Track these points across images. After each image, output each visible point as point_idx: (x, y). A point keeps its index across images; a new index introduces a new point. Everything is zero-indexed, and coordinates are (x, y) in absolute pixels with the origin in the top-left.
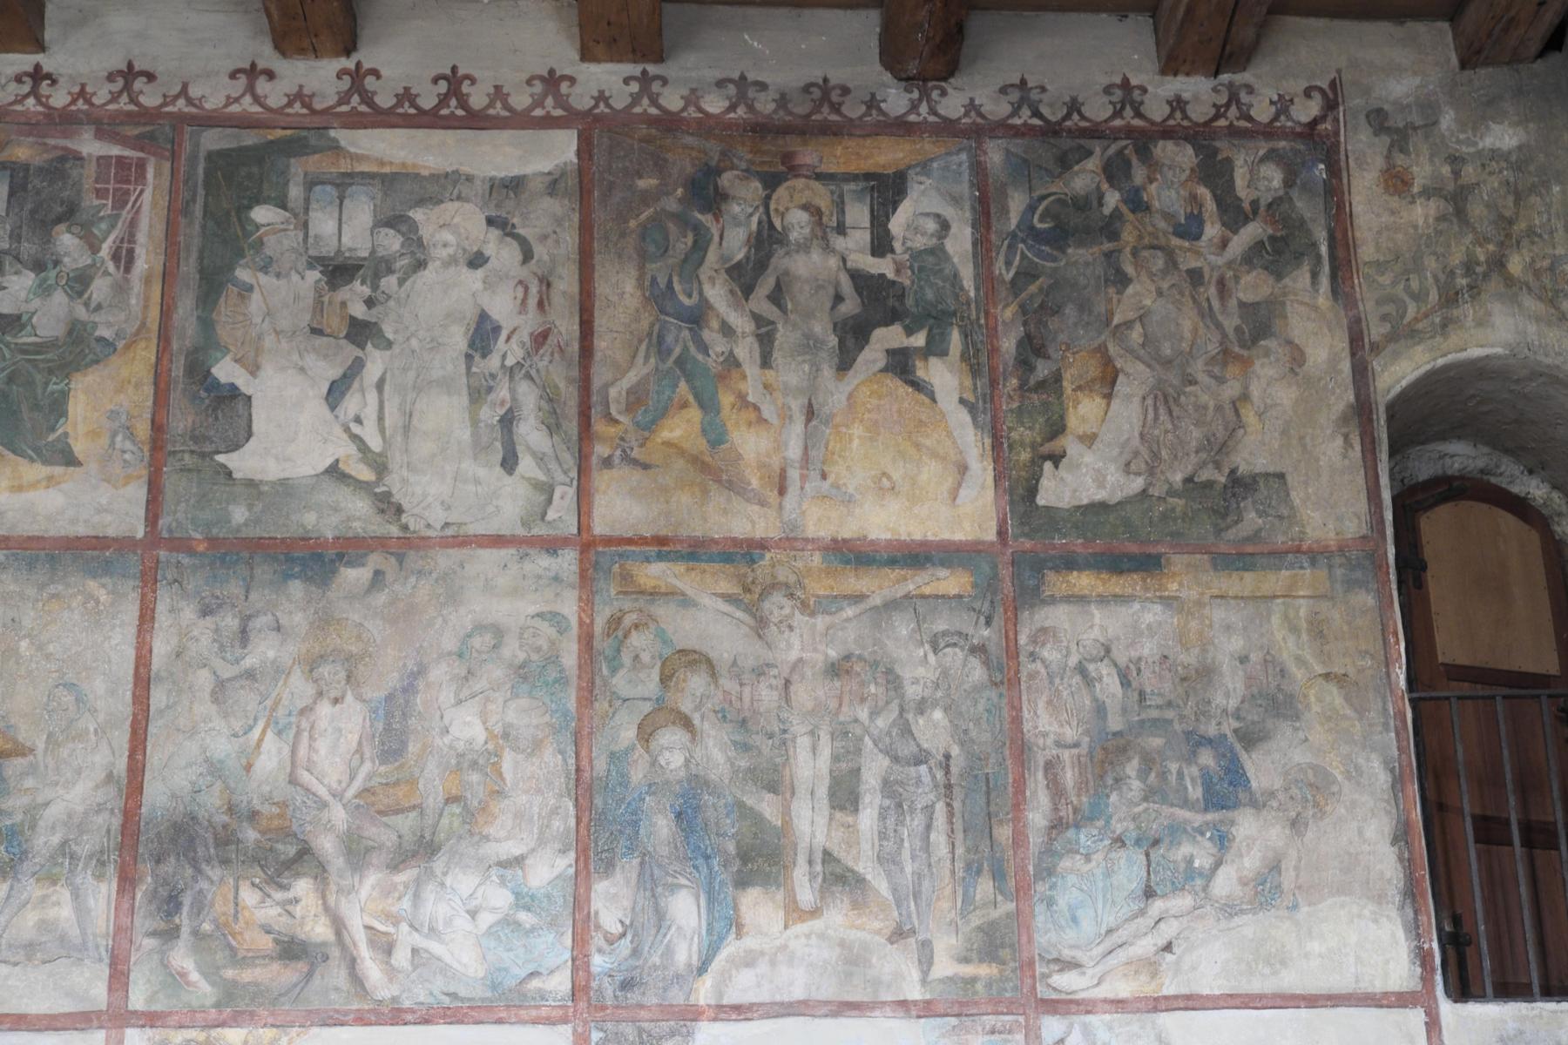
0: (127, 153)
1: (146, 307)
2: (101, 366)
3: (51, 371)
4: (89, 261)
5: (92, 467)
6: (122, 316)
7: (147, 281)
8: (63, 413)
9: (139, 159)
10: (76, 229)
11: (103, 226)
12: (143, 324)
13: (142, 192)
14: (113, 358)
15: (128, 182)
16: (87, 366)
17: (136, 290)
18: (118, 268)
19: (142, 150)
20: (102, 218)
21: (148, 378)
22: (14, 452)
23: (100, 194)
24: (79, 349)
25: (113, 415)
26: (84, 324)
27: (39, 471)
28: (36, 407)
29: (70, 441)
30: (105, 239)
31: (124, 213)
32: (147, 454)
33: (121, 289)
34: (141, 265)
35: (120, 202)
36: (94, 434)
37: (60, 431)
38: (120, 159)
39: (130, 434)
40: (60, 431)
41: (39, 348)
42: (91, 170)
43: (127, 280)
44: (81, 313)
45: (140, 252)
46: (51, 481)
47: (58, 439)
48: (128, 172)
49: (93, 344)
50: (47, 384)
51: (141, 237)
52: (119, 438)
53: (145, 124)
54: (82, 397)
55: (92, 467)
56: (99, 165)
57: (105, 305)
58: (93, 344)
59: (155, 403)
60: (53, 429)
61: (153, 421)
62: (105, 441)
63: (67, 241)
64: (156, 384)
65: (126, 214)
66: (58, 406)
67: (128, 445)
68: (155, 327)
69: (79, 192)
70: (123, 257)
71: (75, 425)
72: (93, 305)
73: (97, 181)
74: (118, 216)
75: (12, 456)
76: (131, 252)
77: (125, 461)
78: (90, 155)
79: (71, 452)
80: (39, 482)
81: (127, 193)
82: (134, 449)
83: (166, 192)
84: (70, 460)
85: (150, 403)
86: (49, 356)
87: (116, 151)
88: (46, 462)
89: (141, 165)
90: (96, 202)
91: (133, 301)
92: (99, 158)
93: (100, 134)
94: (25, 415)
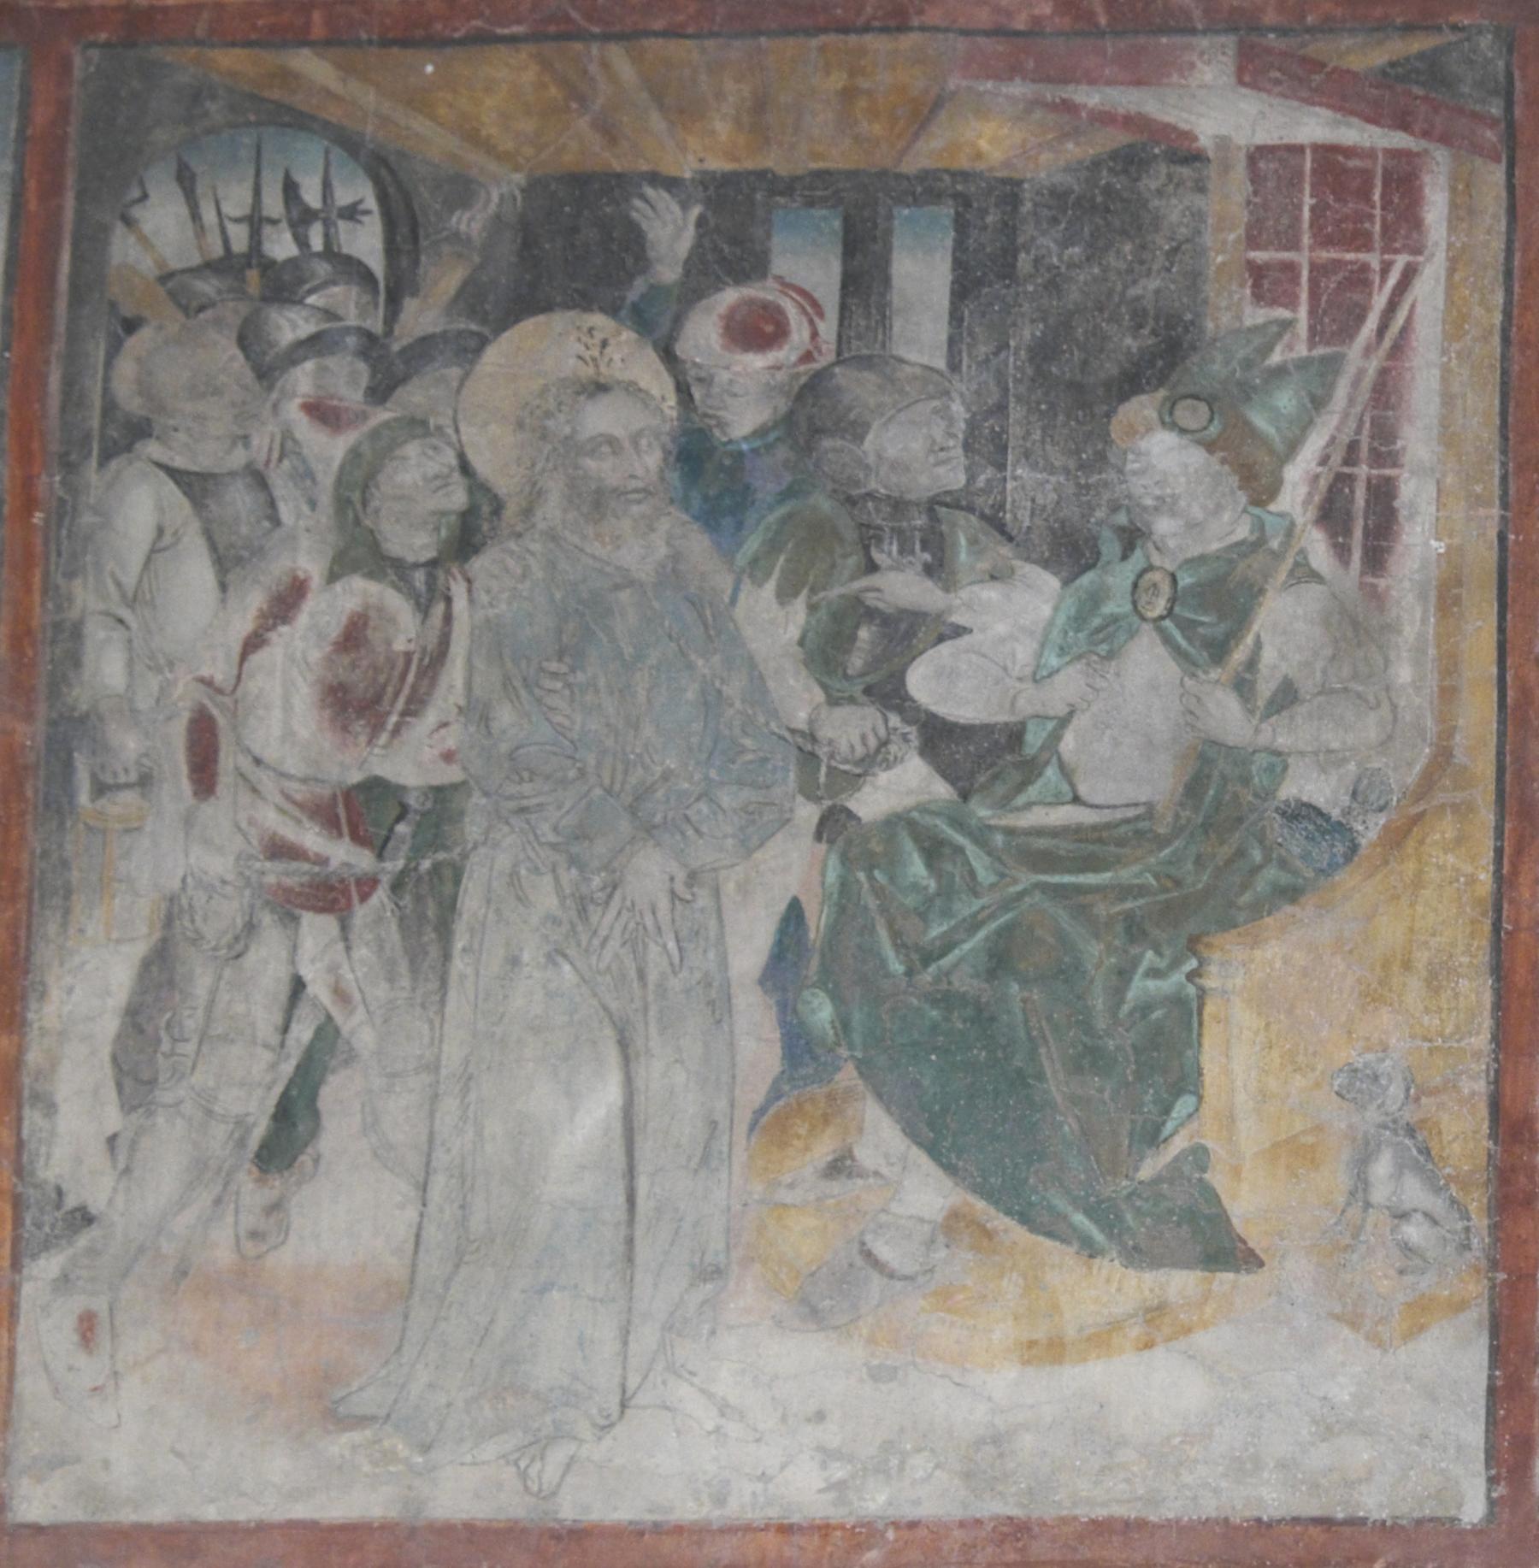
0: (1354, 134)
1: (1448, 694)
2: (1305, 910)
3: (1134, 930)
4: (1243, 532)
5: (1295, 1270)
6: (1371, 728)
7: (1447, 597)
8: (1185, 1081)
9: (1394, 154)
10: (1192, 415)
11: (1286, 400)
12: (1443, 755)
13: (1409, 274)
14: (1346, 878)
15: (1360, 240)
16: (1258, 910)
17: (1410, 632)
18: (1342, 552)
19: (1403, 123)
20: (1280, 371)
21: (1470, 953)
22: (1025, 1219)
23: (1268, 283)
24: (1225, 849)
25: (1357, 1085)
26: (1240, 757)
27: (1106, 1288)
28: (1090, 1058)
29: (1217, 1178)
30: (1293, 447)
31: (1355, 351)
32: (1480, 1222)
33: (1358, 629)
34: (1420, 542)
35: (1338, 314)
36: (1295, 1153)
37: (1179, 1144)
38: (1327, 154)
39: (1423, 1154)
40: (1179, 1144)
41: (1093, 846)
42: (1231, 196)
43: (1376, 597)
44: (1228, 717)
45: (1416, 494)
46: (1157, 1324)
47: (1173, 1173)
48: (1359, 206)
49: (1277, 828)
50: (1124, 975)
51: (1418, 442)
52: (1382, 1167)
53: (1408, 29)
54: (1244, 1017)
55: (1295, 1270)
56: (1256, 178)
57: (1306, 686)
58: (1277, 828)
59: (1502, 1039)
60: (1153, 1137)
61: (1495, 1105)
62: (1335, 1178)
63: (1162, 457)
64: (1500, 971)
65: (1359, 358)
66: (1165, 1058)
67: (1414, 1192)
68: (1484, 767)
69: (1194, 279)
70: (1362, 515)
71: (1229, 1120)
72: (1265, 689)
73: (1253, 240)
74: (1330, 367)
75: (1019, 1234)
76: (1383, 495)
77: (1407, 1248)
78: (1223, 143)
79: (1221, 1219)
80: (1116, 1325)
81: (1359, 279)
82: (1438, 1205)
83: (1492, 278)
84: (1222, 1250)
85: (1481, 1040)
86: (1126, 875)
87: (1314, 127)
88: (1138, 1256)
89: (1403, 181)
90: (1256, 315)
91: (1404, 673)
92: (1257, 154)
93: (1253, 69)
94: (1056, 1084)
